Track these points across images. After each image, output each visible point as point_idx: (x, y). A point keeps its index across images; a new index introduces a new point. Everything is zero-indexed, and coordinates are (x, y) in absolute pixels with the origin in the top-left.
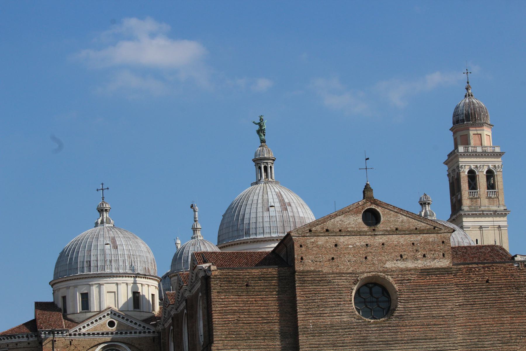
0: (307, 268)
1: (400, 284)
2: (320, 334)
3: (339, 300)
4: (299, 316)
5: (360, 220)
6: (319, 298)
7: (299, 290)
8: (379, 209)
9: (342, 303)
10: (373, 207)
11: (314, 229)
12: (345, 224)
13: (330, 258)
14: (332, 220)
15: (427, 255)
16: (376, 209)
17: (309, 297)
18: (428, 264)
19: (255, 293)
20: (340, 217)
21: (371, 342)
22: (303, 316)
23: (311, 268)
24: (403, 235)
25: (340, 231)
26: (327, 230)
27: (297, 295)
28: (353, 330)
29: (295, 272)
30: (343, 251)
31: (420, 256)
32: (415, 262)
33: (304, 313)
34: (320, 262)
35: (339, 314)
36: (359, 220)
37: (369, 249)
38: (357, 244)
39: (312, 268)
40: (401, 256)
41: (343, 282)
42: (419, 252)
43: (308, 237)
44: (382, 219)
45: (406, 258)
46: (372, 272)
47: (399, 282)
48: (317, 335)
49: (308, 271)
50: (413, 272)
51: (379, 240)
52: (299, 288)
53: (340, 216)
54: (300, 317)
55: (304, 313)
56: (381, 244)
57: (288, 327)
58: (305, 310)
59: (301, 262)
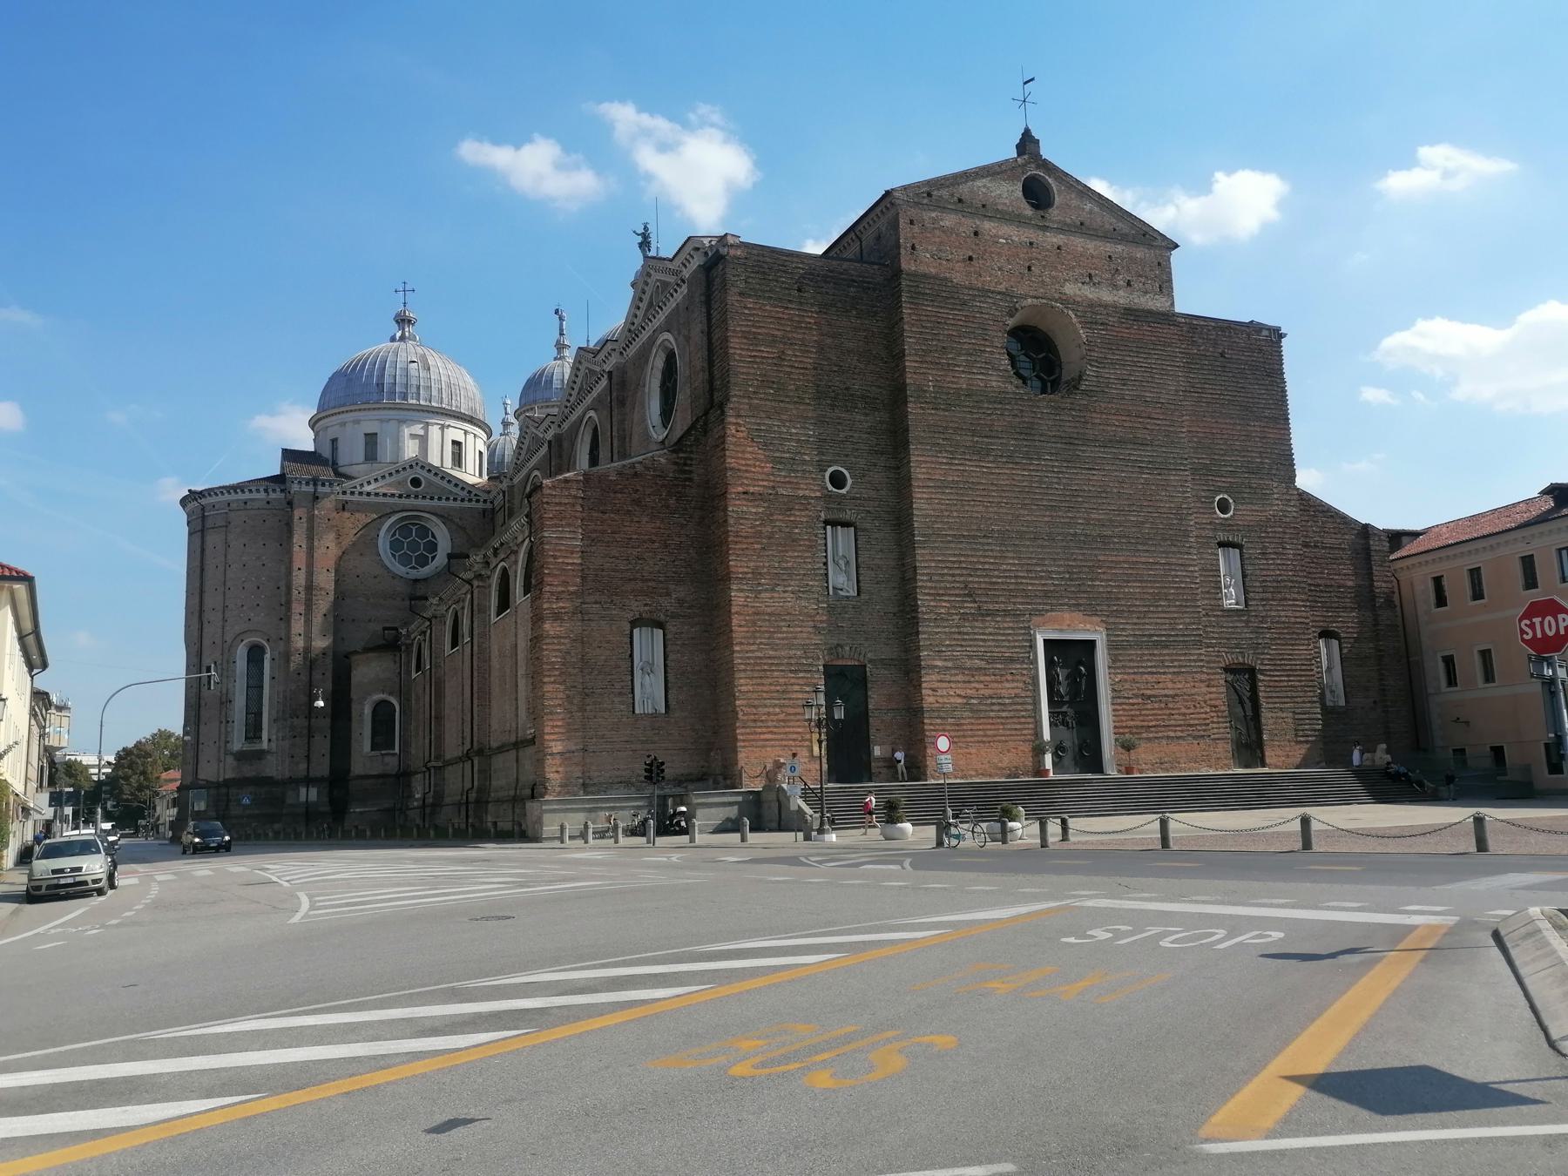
0: (922, 269)
1: (1088, 330)
5: (1020, 194)
7: (910, 311)
11: (935, 193)
13: (966, 257)
16: (1047, 177)
23: (932, 270)
26: (960, 201)
27: (906, 320)
29: (898, 273)
30: (990, 247)
31: (1122, 283)
32: (1115, 292)
36: (1018, 192)
38: (1014, 238)
40: (1090, 276)
49: (925, 276)
54: (910, 363)
57: (880, 387)
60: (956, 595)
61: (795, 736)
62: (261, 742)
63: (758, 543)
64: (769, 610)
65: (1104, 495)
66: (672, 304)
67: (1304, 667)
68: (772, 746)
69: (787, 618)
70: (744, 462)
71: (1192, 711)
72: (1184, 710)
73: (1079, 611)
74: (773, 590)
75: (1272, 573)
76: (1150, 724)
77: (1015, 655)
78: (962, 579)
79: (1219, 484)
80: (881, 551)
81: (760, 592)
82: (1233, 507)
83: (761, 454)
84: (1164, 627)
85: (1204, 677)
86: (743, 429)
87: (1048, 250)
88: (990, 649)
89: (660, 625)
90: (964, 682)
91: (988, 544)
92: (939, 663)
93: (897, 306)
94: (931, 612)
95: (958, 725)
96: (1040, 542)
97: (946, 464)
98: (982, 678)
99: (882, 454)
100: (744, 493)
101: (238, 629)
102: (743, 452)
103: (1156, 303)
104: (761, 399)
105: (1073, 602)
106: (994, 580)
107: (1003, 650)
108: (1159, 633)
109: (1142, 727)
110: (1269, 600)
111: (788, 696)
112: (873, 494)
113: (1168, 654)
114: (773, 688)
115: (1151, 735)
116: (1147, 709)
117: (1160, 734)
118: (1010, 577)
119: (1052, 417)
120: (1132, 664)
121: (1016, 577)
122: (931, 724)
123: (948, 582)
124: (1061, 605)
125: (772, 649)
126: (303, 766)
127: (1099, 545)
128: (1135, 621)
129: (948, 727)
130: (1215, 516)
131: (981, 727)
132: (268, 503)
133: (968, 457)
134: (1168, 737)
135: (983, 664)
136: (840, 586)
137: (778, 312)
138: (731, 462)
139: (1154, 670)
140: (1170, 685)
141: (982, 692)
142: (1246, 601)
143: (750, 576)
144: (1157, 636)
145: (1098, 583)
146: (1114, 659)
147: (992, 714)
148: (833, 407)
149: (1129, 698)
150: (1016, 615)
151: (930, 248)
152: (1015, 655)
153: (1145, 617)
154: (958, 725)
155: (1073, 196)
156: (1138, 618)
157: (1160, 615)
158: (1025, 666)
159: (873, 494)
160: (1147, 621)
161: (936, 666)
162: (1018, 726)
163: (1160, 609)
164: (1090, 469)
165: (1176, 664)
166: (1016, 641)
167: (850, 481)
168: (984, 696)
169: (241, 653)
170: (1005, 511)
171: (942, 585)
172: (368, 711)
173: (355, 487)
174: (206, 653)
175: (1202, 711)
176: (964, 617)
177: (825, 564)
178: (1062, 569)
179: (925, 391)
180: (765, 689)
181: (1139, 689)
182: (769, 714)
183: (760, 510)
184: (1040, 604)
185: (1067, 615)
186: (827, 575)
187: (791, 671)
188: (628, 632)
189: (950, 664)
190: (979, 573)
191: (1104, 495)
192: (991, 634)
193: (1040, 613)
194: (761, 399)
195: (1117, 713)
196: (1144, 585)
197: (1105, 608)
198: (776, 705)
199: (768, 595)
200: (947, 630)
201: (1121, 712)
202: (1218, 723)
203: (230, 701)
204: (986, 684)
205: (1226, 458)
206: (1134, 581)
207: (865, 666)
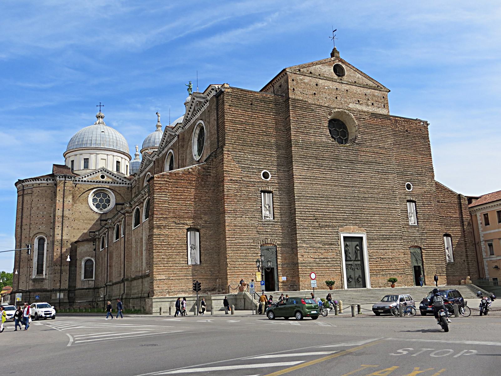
0: (297, 97)
3: (319, 125)
6: (306, 121)
7: (292, 113)
8: (344, 66)
9: (321, 127)
10: (340, 64)
11: (302, 70)
12: (323, 71)
13: (313, 93)
14: (314, 66)
15: (375, 104)
17: (299, 119)
19: (258, 111)
21: (342, 159)
22: (295, 132)
24: (359, 88)
25: (319, 75)
26: (311, 73)
27: (291, 116)
28: (329, 149)
29: (288, 98)
31: (370, 104)
33: (295, 130)
35: (320, 135)
38: (330, 87)
39: (301, 98)
40: (359, 101)
41: (321, 112)
43: (298, 75)
47: (358, 119)
48: (305, 148)
50: (366, 114)
52: (292, 111)
53: (319, 64)
55: (295, 130)
56: (346, 90)
58: (296, 128)
59: (293, 92)
61: (249, 273)
62: (43, 275)
64: (240, 225)
66: (203, 110)
72: (396, 263)
74: (241, 217)
77: (332, 242)
85: (403, 251)
89: (198, 230)
92: (305, 245)
94: (301, 226)
95: (311, 269)
98: (320, 251)
100: (230, 180)
101: (35, 232)
103: (383, 112)
105: (354, 222)
106: (325, 214)
108: (386, 234)
117: (387, 273)
126: (58, 285)
128: (377, 229)
132: (48, 184)
134: (390, 274)
135: (321, 246)
136: (267, 216)
139: (384, 248)
140: (390, 254)
141: (321, 256)
142: (418, 222)
144: (385, 235)
152: (332, 242)
154: (311, 269)
156: (378, 228)
160: (382, 229)
162: (334, 270)
167: (270, 176)
169: (36, 241)
172: (83, 263)
173: (80, 179)
174: (23, 241)
176: (314, 228)
177: (261, 207)
186: (262, 211)
188: (186, 233)
189: (308, 246)
190: (319, 211)
192: (323, 234)
195: (371, 265)
199: (240, 219)
201: (372, 264)
203: (32, 260)
204: (322, 253)
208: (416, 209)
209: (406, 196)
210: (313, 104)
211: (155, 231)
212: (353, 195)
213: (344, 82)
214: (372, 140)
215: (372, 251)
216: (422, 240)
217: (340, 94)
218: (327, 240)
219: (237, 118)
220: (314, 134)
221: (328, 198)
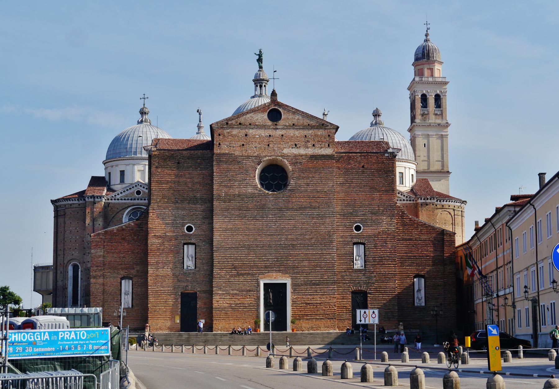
2: (230, 201)
4: (214, 187)
7: (216, 168)
10: (277, 108)
11: (230, 122)
12: (254, 119)
14: (244, 116)
16: (279, 109)
18: (316, 152)
20: (251, 114)
25: (250, 124)
26: (240, 124)
29: (213, 154)
31: (310, 145)
32: (307, 150)
34: (233, 147)
36: (265, 116)
37: (271, 139)
39: (227, 152)
40: (296, 145)
42: (310, 142)
44: (283, 117)
45: (299, 147)
46: (273, 156)
49: (224, 154)
50: (304, 157)
51: (279, 132)
53: (250, 113)
54: (215, 187)
57: (208, 195)
60: (229, 268)
63: (159, 252)
64: (161, 275)
65: (295, 229)
67: (391, 291)
68: (160, 319)
69: (168, 277)
70: (154, 225)
71: (328, 309)
72: (324, 309)
73: (280, 272)
74: (163, 268)
75: (379, 254)
76: (308, 314)
77: (251, 289)
78: (231, 262)
79: (356, 220)
80: (205, 253)
81: (159, 269)
82: (362, 228)
83: (161, 222)
84: (318, 277)
86: (155, 214)
87: (277, 137)
88: (241, 287)
90: (230, 299)
91: (243, 250)
92: (220, 292)
93: (212, 166)
94: (218, 274)
95: (226, 313)
96: (265, 248)
97: (228, 222)
98: (237, 297)
99: (207, 218)
100: (154, 236)
102: (154, 222)
104: (162, 203)
105: (278, 269)
106: (245, 262)
107: (246, 287)
109: (305, 314)
110: (376, 265)
111: (167, 303)
112: (203, 233)
113: (319, 288)
114: (162, 300)
115: (308, 318)
116: (307, 308)
117: (312, 317)
118: (252, 261)
119: (274, 201)
120: (302, 292)
121: (254, 261)
122: (215, 313)
123: (226, 264)
124: (273, 270)
125: (162, 288)
127: (291, 248)
129: (222, 314)
130: (353, 232)
131: (235, 314)
133: (236, 219)
134: (316, 319)
136: (189, 266)
137: (170, 172)
138: (150, 226)
139: (312, 294)
141: (237, 302)
143: (155, 263)
145: (289, 262)
146: (294, 291)
147: (240, 310)
148: (189, 203)
149: (299, 304)
150: (253, 275)
151: (226, 143)
152: (251, 289)
153: (309, 274)
154: (226, 313)
155: (290, 114)
156: (306, 274)
157: (316, 273)
158: (255, 293)
159: (203, 233)
161: (219, 293)
162: (251, 314)
163: (317, 271)
164: (290, 219)
165: (322, 291)
166: (252, 284)
167: (194, 229)
168: (237, 304)
170: (251, 237)
171: (223, 265)
175: (333, 309)
178: (274, 257)
179: (221, 196)
180: (158, 301)
181: (304, 301)
182: (160, 309)
183: (160, 241)
184: (263, 270)
185: (274, 274)
187: (169, 295)
189: (224, 292)
190: (238, 260)
191: (295, 229)
192: (242, 282)
193: (263, 274)
194: (162, 203)
195: (293, 309)
196: (310, 262)
197: (292, 271)
198: (162, 306)
199: (161, 270)
200: (224, 281)
201: (295, 309)
202: (346, 313)
205: (360, 209)
206: (306, 261)
207: (197, 293)
208: (365, 251)
209: (352, 239)
210: (240, 156)
211: (92, 281)
212: (279, 243)
213: (279, 127)
214: (308, 185)
215: (296, 296)
216: (368, 284)
217: (273, 140)
218: (245, 287)
219: (162, 178)
220: (239, 187)
221: (249, 247)
